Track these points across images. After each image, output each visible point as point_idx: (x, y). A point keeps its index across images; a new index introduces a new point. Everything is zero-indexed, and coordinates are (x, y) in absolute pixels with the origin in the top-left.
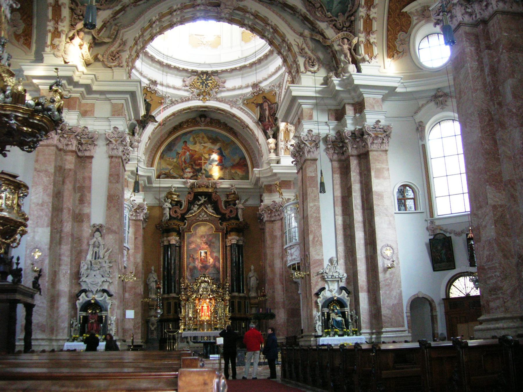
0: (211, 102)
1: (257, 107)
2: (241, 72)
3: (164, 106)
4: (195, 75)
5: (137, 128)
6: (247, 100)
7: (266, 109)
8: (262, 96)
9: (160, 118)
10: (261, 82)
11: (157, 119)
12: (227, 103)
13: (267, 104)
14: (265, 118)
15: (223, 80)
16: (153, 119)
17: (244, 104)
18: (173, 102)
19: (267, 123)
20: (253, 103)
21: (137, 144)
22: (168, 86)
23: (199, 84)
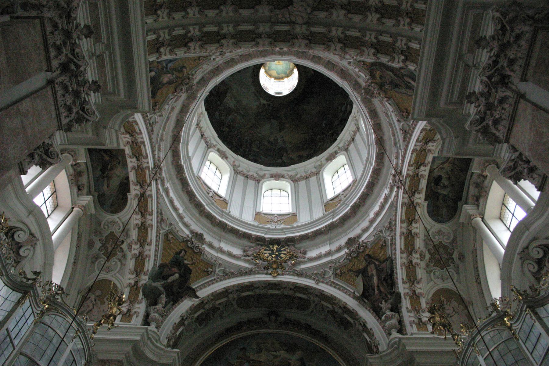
0: (284, 276)
1: (357, 276)
2: (329, 235)
3: (213, 278)
4: (262, 245)
5: (163, 299)
6: (342, 267)
7: (372, 275)
8: (362, 256)
9: (204, 293)
10: (359, 236)
11: (198, 294)
12: (310, 278)
13: (372, 266)
14: (374, 290)
15: (302, 249)
16: (193, 293)
17: (336, 275)
18: (227, 275)
19: (377, 296)
20: (351, 270)
21: (157, 315)
22: (221, 251)
23: (267, 255)
